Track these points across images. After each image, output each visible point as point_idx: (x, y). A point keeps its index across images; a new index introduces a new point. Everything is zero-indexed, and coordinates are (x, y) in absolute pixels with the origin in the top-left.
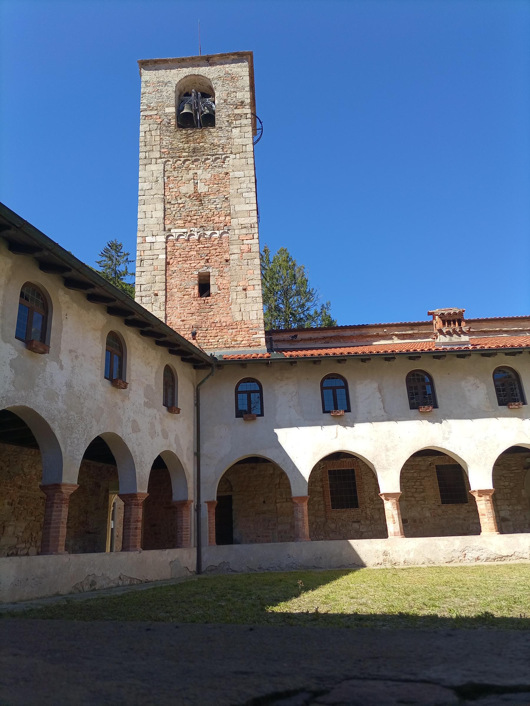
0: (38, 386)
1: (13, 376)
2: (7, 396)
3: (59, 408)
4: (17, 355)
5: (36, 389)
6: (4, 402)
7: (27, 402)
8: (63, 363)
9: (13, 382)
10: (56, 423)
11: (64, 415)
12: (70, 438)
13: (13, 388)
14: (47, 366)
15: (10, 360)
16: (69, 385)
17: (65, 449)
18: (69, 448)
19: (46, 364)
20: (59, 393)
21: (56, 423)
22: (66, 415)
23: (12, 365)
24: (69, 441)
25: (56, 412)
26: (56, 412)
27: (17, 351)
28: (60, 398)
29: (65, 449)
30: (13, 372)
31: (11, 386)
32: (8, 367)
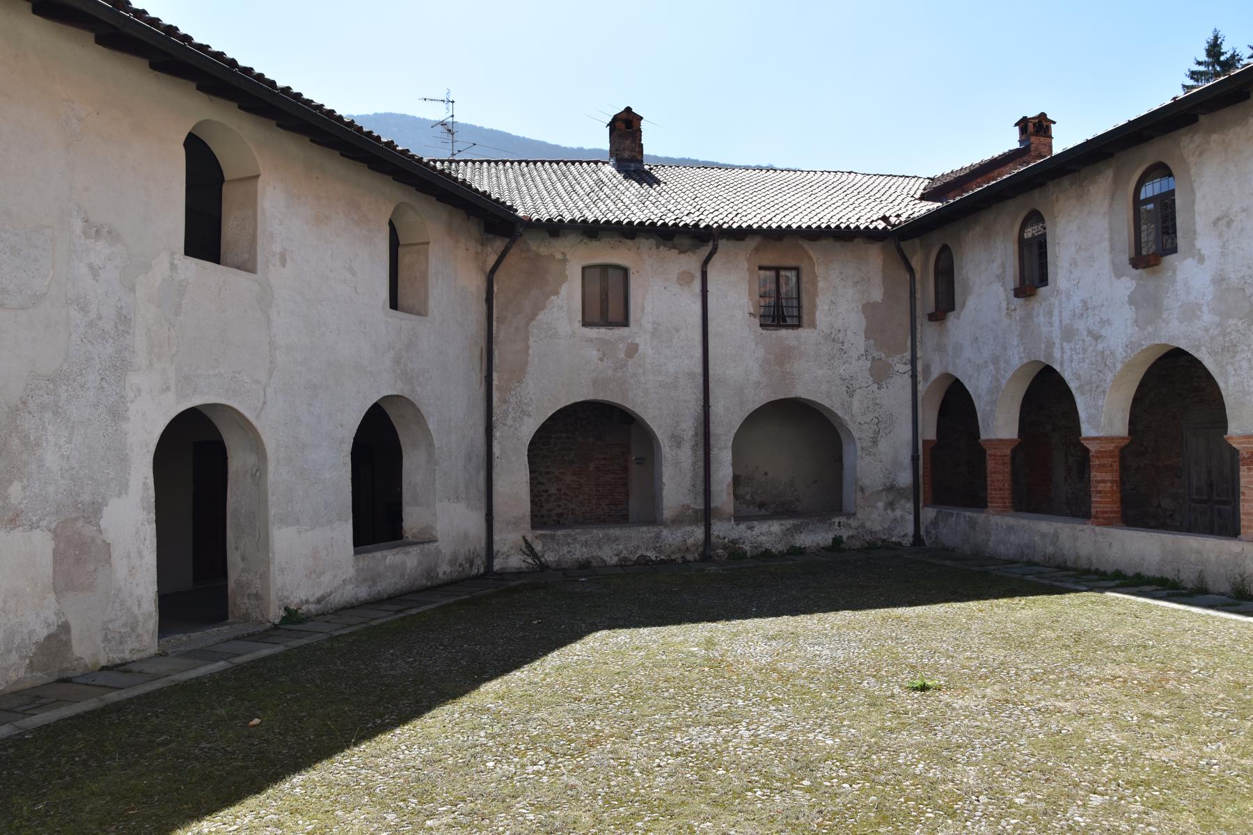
0: (1167, 309)
1: (1134, 315)
2: (1131, 342)
3: (1206, 325)
4: (1135, 284)
5: (1165, 315)
6: (1129, 351)
7: (1156, 338)
8: (1203, 252)
9: (1136, 321)
10: (1204, 349)
11: (1216, 332)
12: (1232, 363)
13: (1137, 328)
14: (1178, 273)
15: (1129, 296)
16: (1220, 280)
17: (1226, 382)
18: (1231, 380)
19: (1174, 272)
20: (1202, 302)
21: (1204, 349)
22: (1219, 329)
23: (1132, 301)
24: (1230, 369)
25: (1201, 333)
26: (1201, 333)
27: (1132, 279)
28: (1205, 308)
29: (1226, 382)
30: (1134, 309)
31: (1135, 327)
32: (1127, 306)
